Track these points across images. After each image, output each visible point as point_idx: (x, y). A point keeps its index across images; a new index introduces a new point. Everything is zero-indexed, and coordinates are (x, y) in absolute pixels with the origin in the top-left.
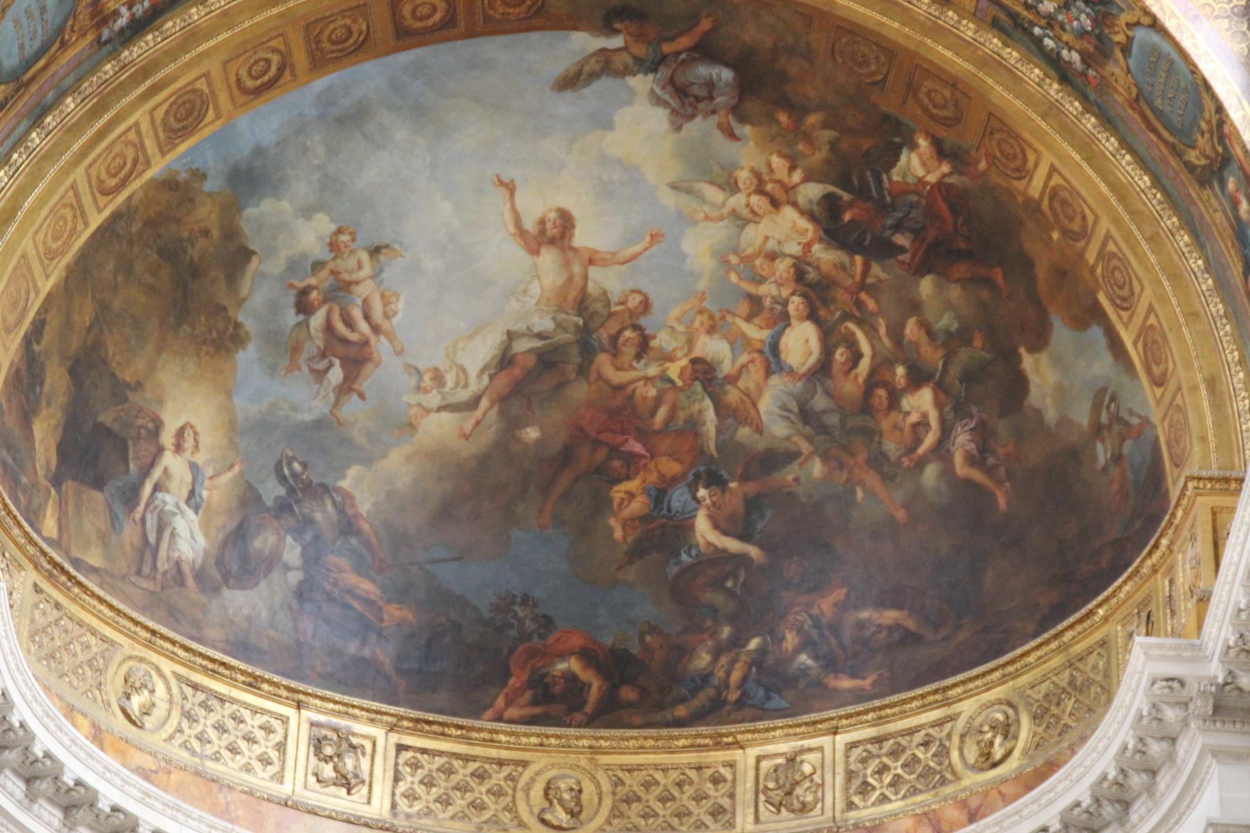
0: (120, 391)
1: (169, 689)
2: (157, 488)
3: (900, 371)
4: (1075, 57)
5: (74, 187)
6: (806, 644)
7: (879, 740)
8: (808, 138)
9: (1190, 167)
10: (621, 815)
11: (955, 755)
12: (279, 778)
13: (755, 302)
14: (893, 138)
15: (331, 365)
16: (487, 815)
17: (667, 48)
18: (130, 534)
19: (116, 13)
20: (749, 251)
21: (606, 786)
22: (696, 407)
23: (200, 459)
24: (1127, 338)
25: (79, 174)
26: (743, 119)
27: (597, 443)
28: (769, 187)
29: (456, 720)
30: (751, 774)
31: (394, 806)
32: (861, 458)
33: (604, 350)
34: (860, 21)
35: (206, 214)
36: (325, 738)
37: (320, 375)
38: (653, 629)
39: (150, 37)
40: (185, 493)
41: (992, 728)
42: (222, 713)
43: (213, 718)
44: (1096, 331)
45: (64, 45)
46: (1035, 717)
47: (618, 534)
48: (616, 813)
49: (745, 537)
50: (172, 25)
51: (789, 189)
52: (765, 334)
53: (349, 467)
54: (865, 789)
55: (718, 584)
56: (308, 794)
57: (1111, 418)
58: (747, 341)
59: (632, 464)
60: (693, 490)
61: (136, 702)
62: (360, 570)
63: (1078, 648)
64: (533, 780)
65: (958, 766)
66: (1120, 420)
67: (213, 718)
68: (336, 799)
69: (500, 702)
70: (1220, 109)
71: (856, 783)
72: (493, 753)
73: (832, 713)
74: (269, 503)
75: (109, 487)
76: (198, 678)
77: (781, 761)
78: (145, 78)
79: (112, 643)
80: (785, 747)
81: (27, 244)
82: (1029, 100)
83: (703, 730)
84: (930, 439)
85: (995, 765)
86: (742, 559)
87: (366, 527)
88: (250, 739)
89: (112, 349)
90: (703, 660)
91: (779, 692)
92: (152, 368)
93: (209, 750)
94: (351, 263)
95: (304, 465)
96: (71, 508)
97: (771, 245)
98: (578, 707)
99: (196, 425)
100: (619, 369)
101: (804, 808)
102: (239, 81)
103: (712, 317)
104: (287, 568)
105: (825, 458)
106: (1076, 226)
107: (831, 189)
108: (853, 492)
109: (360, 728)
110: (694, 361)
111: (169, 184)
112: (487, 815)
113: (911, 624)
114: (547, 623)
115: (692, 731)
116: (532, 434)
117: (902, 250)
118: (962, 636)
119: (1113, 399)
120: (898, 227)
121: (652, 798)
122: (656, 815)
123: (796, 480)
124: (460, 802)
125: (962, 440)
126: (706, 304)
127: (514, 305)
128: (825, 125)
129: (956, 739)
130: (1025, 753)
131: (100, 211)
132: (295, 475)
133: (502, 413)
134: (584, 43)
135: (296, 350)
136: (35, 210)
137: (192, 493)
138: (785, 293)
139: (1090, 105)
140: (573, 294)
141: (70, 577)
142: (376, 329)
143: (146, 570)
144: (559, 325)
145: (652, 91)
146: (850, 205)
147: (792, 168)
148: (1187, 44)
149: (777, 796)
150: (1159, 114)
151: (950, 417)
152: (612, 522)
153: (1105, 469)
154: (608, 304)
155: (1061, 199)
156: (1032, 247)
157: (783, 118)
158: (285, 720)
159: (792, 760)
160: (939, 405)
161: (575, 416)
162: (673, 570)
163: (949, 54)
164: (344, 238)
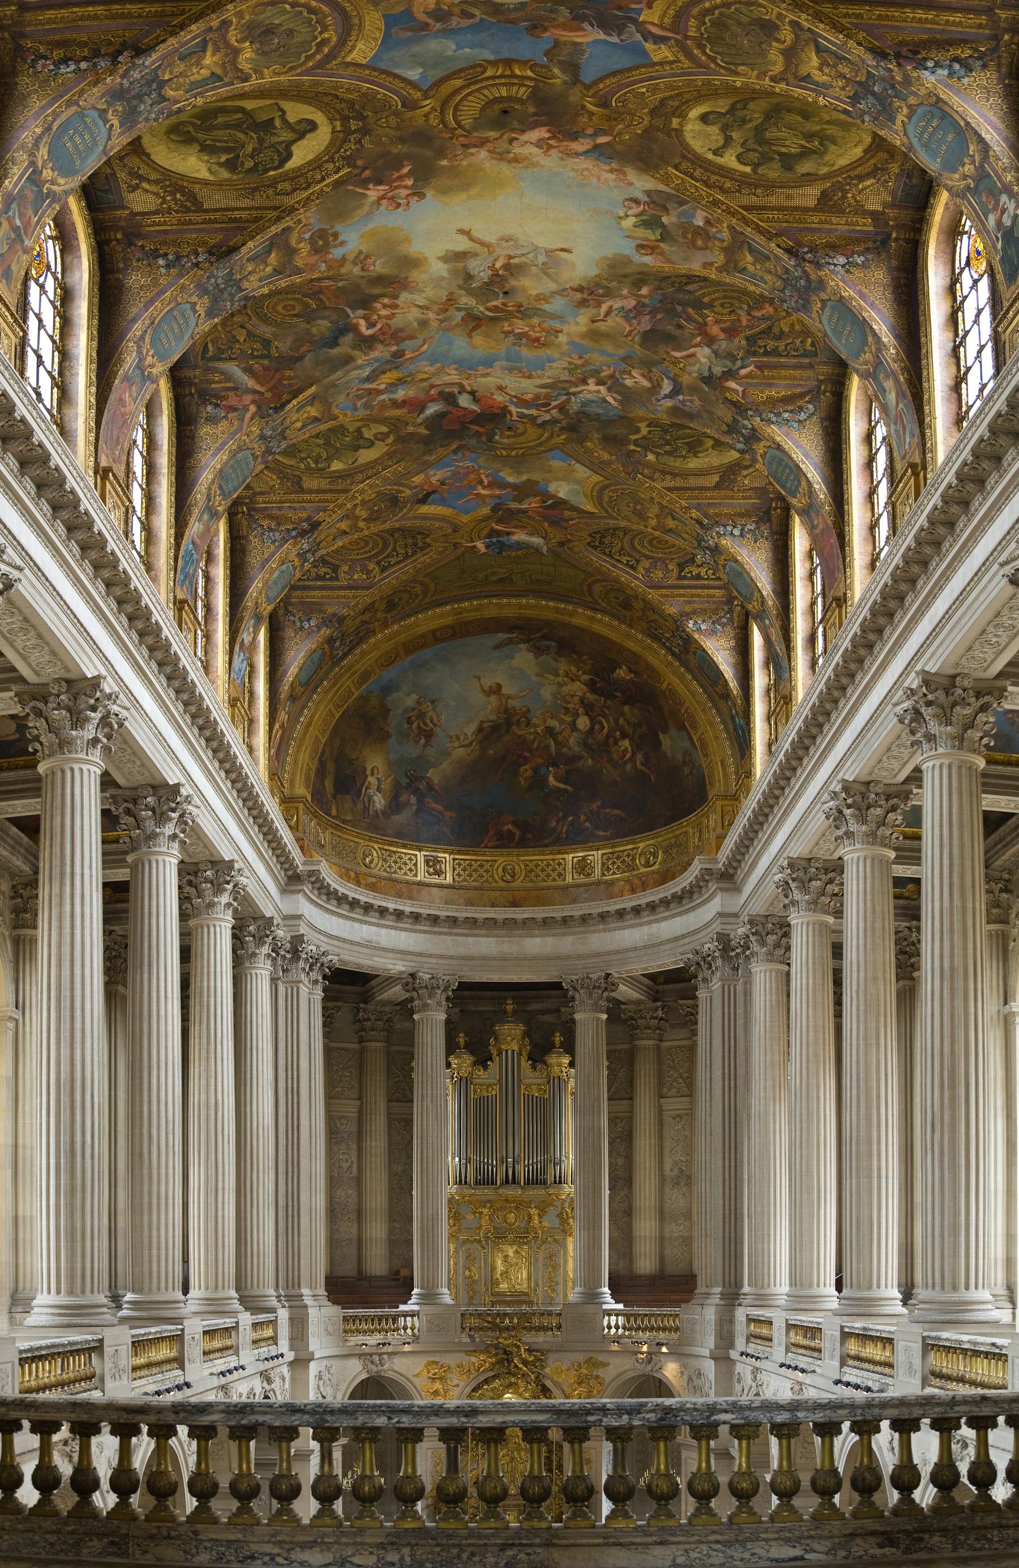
12: (416, 875)
18: (360, 806)
48: (526, 876)
68: (435, 880)
88: (405, 864)
99: (377, 768)
101: (589, 875)
111: (361, 697)
124: (475, 876)
155: (673, 693)
159: (584, 858)
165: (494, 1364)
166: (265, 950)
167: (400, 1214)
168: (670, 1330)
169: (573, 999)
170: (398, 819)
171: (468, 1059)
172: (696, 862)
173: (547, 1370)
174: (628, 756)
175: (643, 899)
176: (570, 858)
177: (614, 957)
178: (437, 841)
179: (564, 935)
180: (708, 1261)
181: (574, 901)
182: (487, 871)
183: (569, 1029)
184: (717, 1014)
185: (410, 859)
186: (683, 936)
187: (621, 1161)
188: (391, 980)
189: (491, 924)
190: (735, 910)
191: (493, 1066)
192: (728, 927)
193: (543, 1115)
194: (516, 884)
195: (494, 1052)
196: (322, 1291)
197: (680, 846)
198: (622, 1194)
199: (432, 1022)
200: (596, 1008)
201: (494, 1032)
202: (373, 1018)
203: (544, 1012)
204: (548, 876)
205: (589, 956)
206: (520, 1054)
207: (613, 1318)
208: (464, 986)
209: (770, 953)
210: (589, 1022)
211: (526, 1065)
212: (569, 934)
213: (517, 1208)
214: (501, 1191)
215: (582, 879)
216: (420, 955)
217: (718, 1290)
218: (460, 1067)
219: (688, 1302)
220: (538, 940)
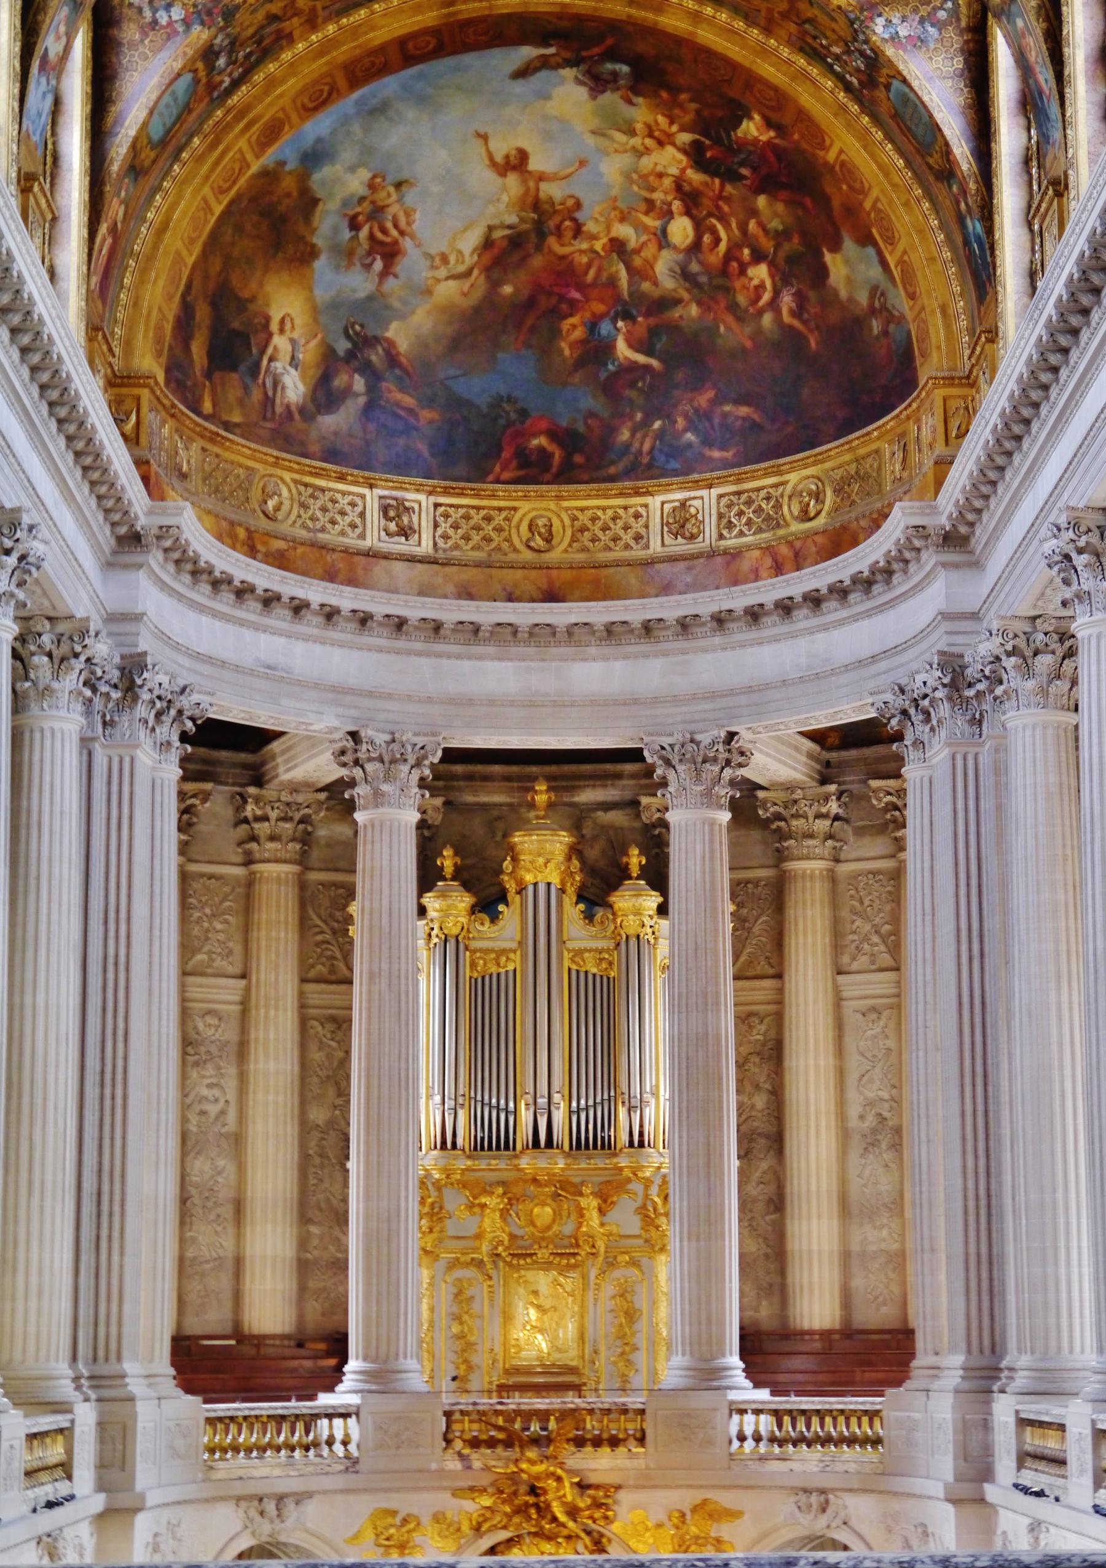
0: (242, 305)
1: (290, 491)
2: (271, 360)
3: (746, 251)
4: (855, 81)
5: (205, 199)
6: (691, 426)
7: (738, 493)
8: (681, 106)
9: (930, 167)
10: (577, 541)
11: (785, 509)
12: (362, 536)
13: (650, 205)
14: (739, 113)
15: (374, 259)
16: (493, 545)
17: (585, 54)
18: (256, 395)
19: (222, 82)
20: (645, 172)
21: (567, 522)
22: (614, 269)
23: (296, 335)
24: (892, 261)
25: (207, 191)
26: (637, 93)
27: (550, 294)
28: (657, 134)
29: (470, 485)
30: (658, 513)
31: (435, 544)
32: (723, 305)
33: (552, 234)
34: (714, 47)
35: (288, 184)
36: (389, 505)
37: (368, 267)
38: (591, 414)
39: (244, 88)
40: (288, 359)
41: (810, 495)
42: (323, 499)
43: (319, 503)
44: (871, 251)
45: (190, 111)
46: (837, 491)
47: (567, 352)
48: (574, 539)
49: (649, 353)
50: (258, 77)
51: (670, 136)
52: (657, 223)
53: (389, 323)
54: (730, 526)
55: (632, 385)
56: (382, 545)
57: (879, 306)
58: (646, 228)
59: (574, 307)
60: (614, 322)
61: (271, 504)
62: (402, 390)
63: (862, 451)
64: (521, 520)
65: (788, 517)
66: (887, 309)
67: (319, 503)
68: (400, 545)
69: (497, 469)
70: (947, 144)
71: (724, 521)
72: (495, 503)
73: (708, 475)
74: (341, 353)
75: (242, 368)
76: (307, 479)
77: (677, 504)
78: (242, 118)
79: (253, 469)
80: (680, 496)
81: (179, 244)
82: (825, 104)
83: (627, 484)
84: (766, 297)
85: (811, 519)
86: (647, 368)
87: (404, 360)
88: (343, 513)
89: (235, 280)
90: (625, 435)
91: (673, 457)
92: (261, 284)
93: (318, 525)
94: (382, 194)
95: (362, 326)
96: (219, 389)
97: (659, 168)
98: (547, 469)
99: (292, 318)
100: (563, 245)
101: (693, 537)
102: (303, 106)
103: (622, 212)
104: (357, 395)
105: (699, 303)
106: (857, 185)
107: (697, 137)
108: (718, 328)
109: (411, 496)
110: (612, 240)
111: (264, 173)
112: (493, 545)
113: (756, 417)
114: (524, 413)
115: (620, 484)
116: (508, 289)
117: (744, 177)
118: (789, 430)
119: (883, 294)
120: (742, 164)
121: (596, 529)
122: (599, 540)
123: (681, 317)
124: (476, 538)
125: (787, 300)
126: (618, 204)
127: (491, 209)
128: (692, 100)
129: (786, 499)
130: (829, 514)
131: (220, 203)
132: (357, 334)
133: (488, 277)
134: (528, 52)
135: (351, 254)
136: (179, 221)
137: (293, 358)
138: (669, 198)
139: (864, 109)
140: (530, 200)
141: (223, 438)
142: (402, 233)
143: (269, 415)
144: (522, 220)
145: (576, 78)
146: (710, 148)
147: (671, 123)
148: (925, 99)
149: (674, 527)
150: (909, 129)
151: (779, 284)
152: (563, 345)
153: (877, 337)
154: (553, 204)
156: (829, 188)
157: (664, 94)
158: (363, 497)
159: (683, 504)
160: (772, 276)
161: (534, 268)
162: (603, 375)
163: (772, 70)
164: (378, 180)
165: (510, 1517)
166: (71, 680)
167: (319, 1206)
168: (864, 1441)
169: (664, 784)
170: (330, 422)
171: (463, 901)
172: (897, 511)
173: (616, 1527)
174: (766, 297)
175: (797, 584)
176: (659, 503)
177: (742, 700)
178: (402, 466)
179: (646, 656)
180: (940, 1314)
181: (666, 589)
182: (499, 530)
183: (656, 841)
184: (943, 811)
185: (353, 505)
186: (874, 658)
187: (760, 1101)
188: (312, 742)
189: (508, 634)
190: (973, 606)
191: (509, 914)
192: (960, 639)
193: (603, 1005)
194: (555, 555)
195: (511, 886)
196: (164, 1367)
197: (860, 477)
198: (764, 1166)
199: (391, 822)
200: (709, 798)
201: (512, 848)
202: (273, 815)
203: (607, 806)
204: (615, 539)
205: (694, 698)
206: (563, 891)
207: (749, 1418)
208: (451, 755)
209: (1044, 692)
210: (696, 829)
211: (573, 911)
212: (656, 655)
213: (556, 1196)
214: (524, 1162)
215: (680, 546)
216: (371, 694)
217: (958, 1359)
218: (445, 913)
219: (898, 1383)
220: (596, 667)
